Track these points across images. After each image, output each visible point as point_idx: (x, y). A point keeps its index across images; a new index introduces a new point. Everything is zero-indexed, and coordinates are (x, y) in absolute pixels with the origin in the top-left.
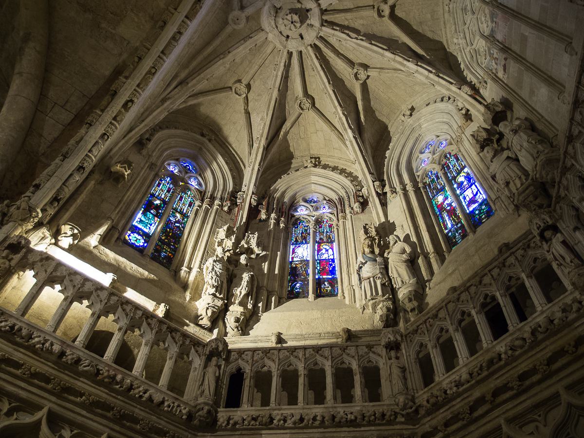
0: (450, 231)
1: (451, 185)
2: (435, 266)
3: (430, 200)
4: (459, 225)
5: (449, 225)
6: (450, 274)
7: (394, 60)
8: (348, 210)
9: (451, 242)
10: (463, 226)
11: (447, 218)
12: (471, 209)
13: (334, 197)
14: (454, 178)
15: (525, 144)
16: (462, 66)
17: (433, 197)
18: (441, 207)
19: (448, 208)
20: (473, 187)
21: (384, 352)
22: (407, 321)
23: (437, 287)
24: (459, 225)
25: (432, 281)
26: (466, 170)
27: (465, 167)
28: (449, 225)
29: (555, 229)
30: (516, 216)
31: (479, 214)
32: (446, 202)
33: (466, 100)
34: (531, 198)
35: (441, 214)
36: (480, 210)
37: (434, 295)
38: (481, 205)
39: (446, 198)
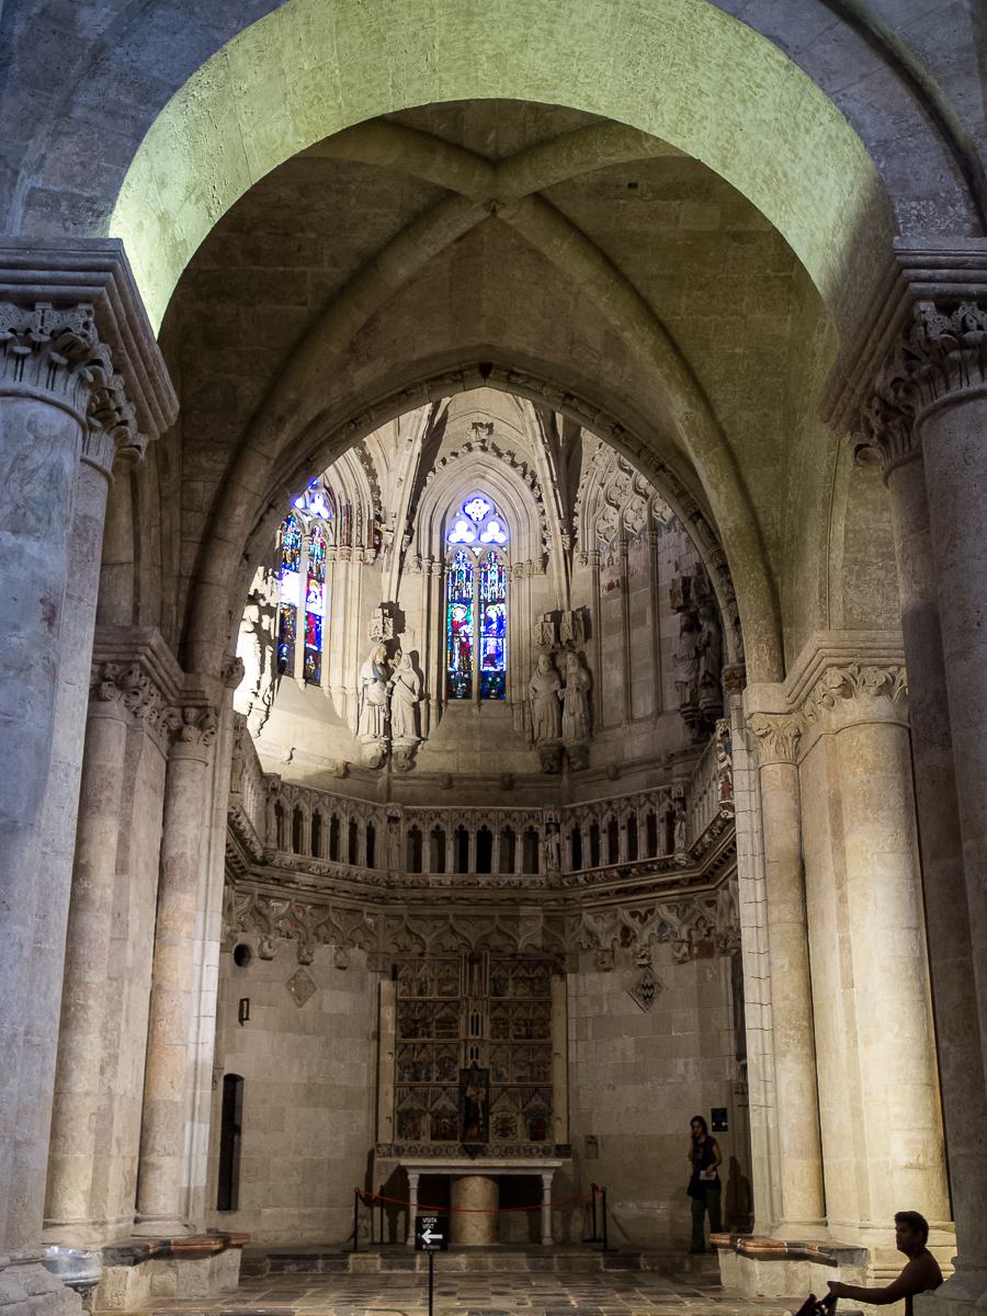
0: (454, 673)
1: (480, 612)
2: (433, 722)
3: (448, 602)
4: (466, 676)
5: (456, 665)
6: (449, 752)
7: (531, 422)
8: (356, 552)
9: (451, 695)
10: (469, 681)
11: (457, 652)
12: (486, 669)
13: (338, 489)
14: (487, 604)
15: (577, 715)
16: (580, 494)
17: (453, 601)
18: (456, 626)
19: (464, 640)
20: (500, 640)
21: (385, 820)
22: (390, 770)
23: (430, 753)
24: (466, 676)
25: (427, 742)
26: (502, 606)
27: (502, 601)
28: (456, 665)
29: (558, 830)
30: (528, 747)
31: (492, 684)
32: (464, 628)
33: (557, 550)
34: (550, 756)
35: (452, 637)
36: (494, 679)
37: (427, 761)
38: (498, 674)
39: (466, 623)
